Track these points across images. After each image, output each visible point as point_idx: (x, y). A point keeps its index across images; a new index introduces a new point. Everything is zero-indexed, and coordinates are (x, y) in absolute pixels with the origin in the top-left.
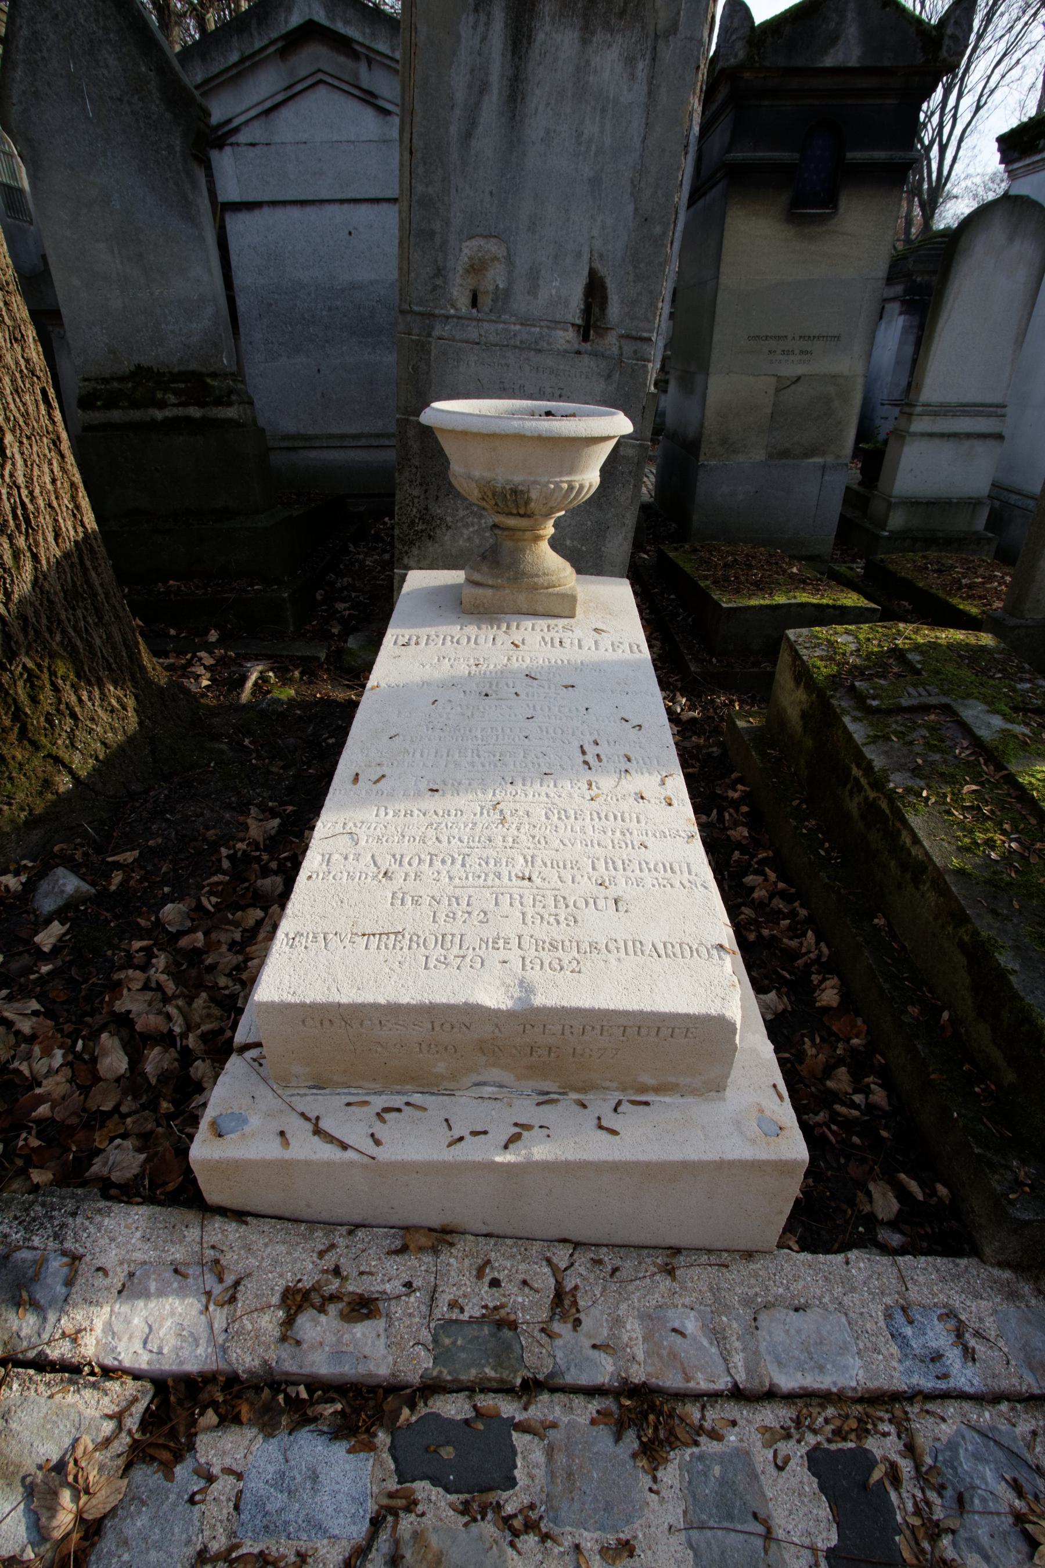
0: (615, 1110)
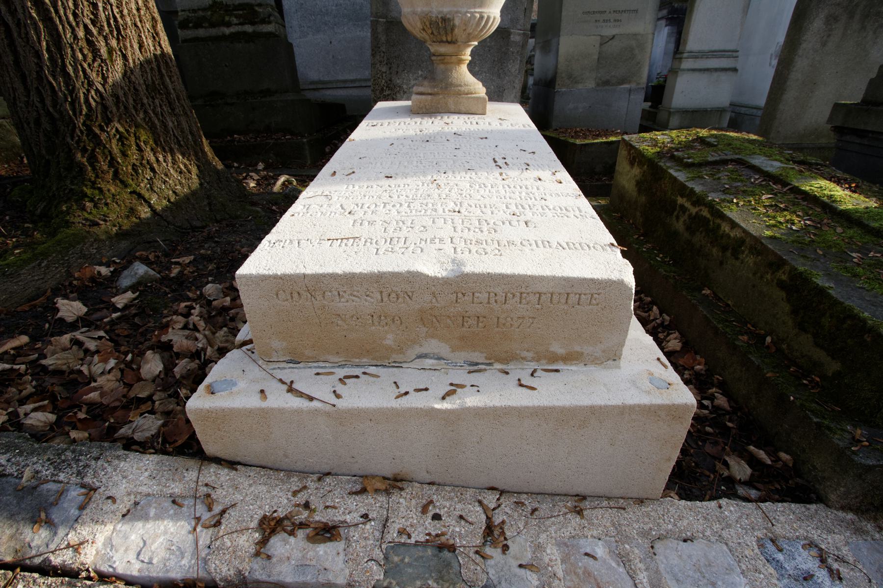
0: (532, 375)
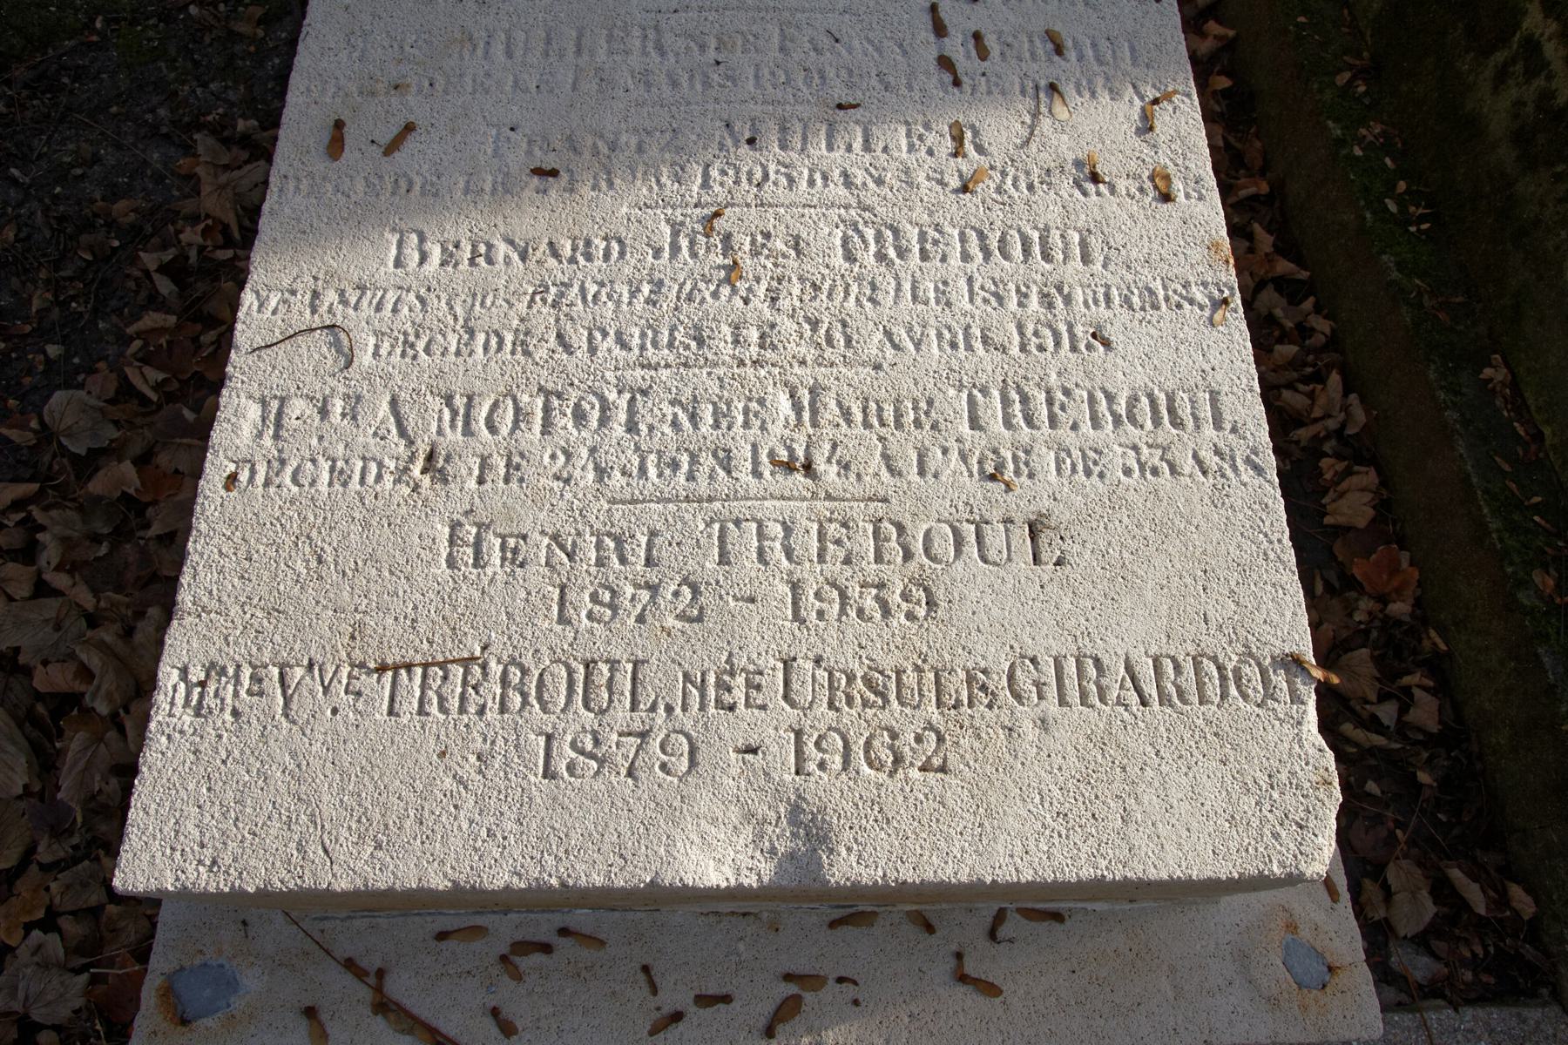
0: (992, 935)
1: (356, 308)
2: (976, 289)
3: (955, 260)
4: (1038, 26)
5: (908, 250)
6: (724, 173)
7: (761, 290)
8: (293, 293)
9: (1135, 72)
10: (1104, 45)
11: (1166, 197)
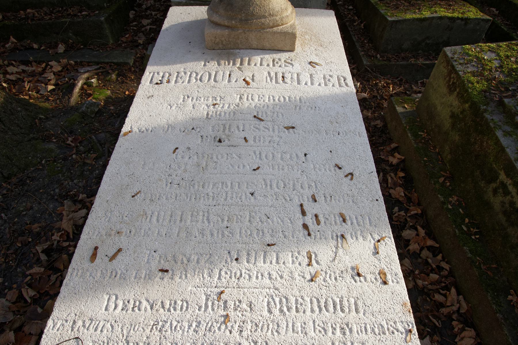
1: (88, 330)
2: (316, 326)
3: (308, 312)
4: (337, 211)
5: (291, 308)
6: (226, 273)
7: (236, 327)
8: (66, 321)
9: (371, 229)
10: (360, 218)
11: (385, 283)
